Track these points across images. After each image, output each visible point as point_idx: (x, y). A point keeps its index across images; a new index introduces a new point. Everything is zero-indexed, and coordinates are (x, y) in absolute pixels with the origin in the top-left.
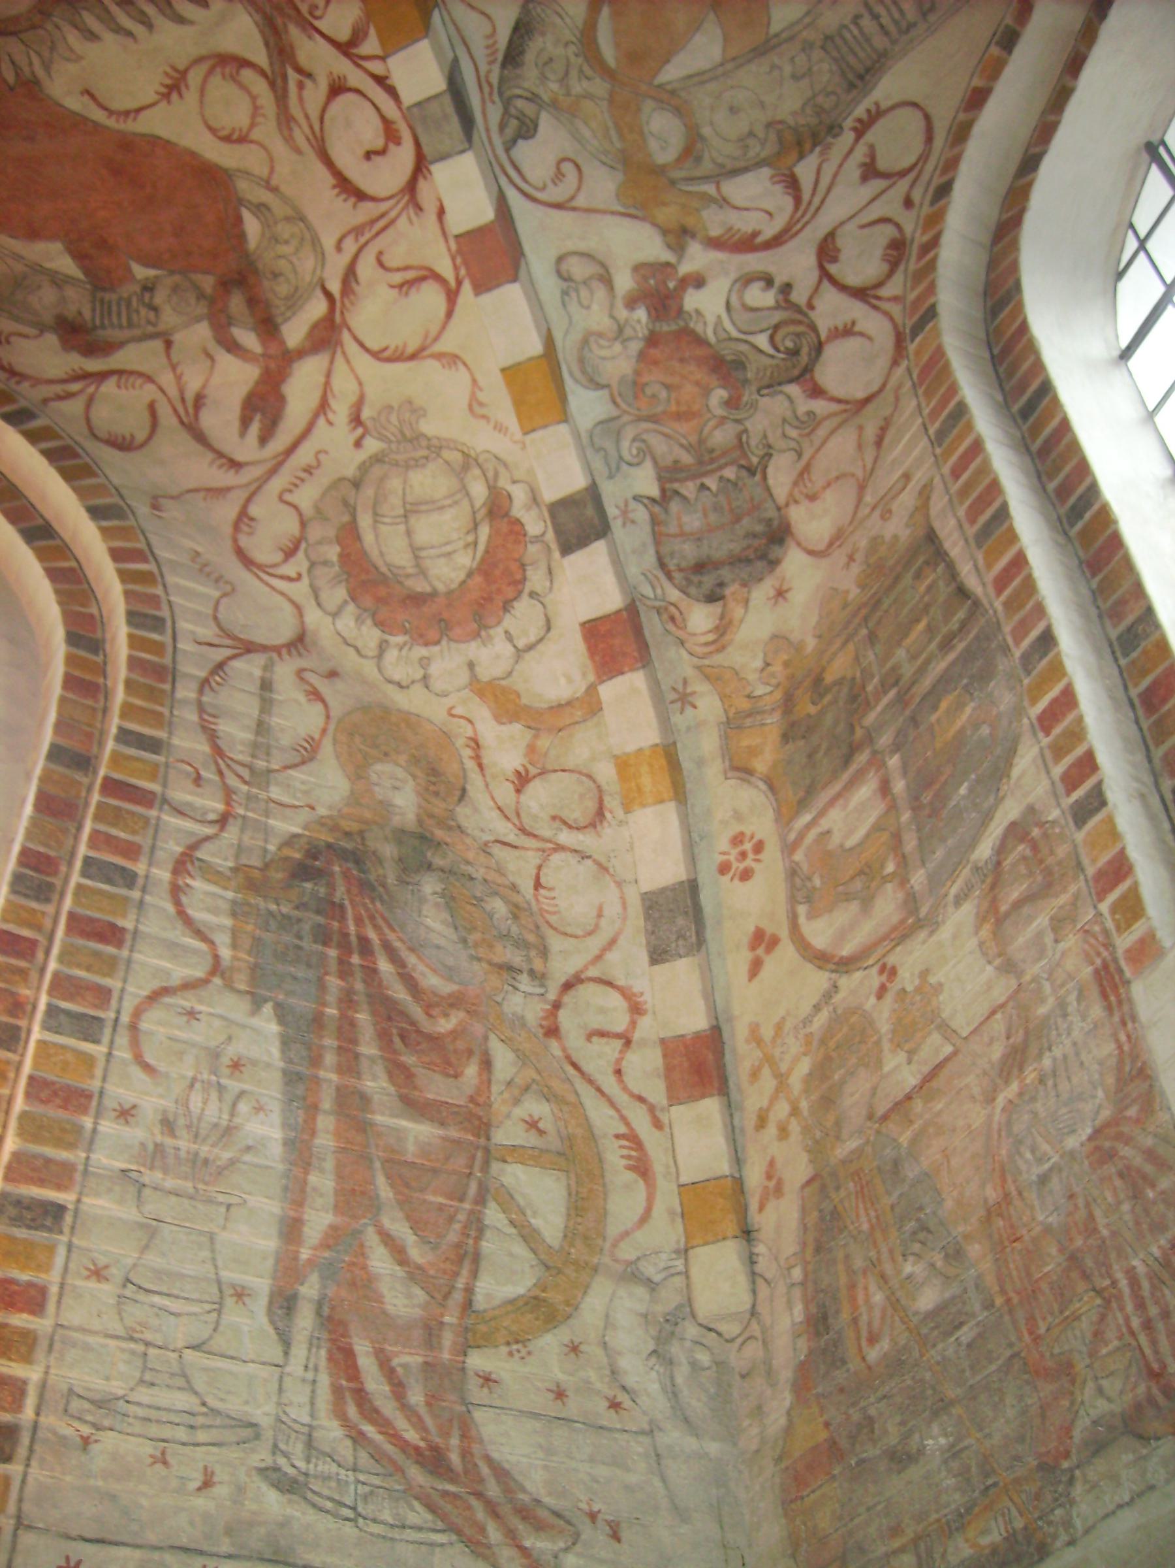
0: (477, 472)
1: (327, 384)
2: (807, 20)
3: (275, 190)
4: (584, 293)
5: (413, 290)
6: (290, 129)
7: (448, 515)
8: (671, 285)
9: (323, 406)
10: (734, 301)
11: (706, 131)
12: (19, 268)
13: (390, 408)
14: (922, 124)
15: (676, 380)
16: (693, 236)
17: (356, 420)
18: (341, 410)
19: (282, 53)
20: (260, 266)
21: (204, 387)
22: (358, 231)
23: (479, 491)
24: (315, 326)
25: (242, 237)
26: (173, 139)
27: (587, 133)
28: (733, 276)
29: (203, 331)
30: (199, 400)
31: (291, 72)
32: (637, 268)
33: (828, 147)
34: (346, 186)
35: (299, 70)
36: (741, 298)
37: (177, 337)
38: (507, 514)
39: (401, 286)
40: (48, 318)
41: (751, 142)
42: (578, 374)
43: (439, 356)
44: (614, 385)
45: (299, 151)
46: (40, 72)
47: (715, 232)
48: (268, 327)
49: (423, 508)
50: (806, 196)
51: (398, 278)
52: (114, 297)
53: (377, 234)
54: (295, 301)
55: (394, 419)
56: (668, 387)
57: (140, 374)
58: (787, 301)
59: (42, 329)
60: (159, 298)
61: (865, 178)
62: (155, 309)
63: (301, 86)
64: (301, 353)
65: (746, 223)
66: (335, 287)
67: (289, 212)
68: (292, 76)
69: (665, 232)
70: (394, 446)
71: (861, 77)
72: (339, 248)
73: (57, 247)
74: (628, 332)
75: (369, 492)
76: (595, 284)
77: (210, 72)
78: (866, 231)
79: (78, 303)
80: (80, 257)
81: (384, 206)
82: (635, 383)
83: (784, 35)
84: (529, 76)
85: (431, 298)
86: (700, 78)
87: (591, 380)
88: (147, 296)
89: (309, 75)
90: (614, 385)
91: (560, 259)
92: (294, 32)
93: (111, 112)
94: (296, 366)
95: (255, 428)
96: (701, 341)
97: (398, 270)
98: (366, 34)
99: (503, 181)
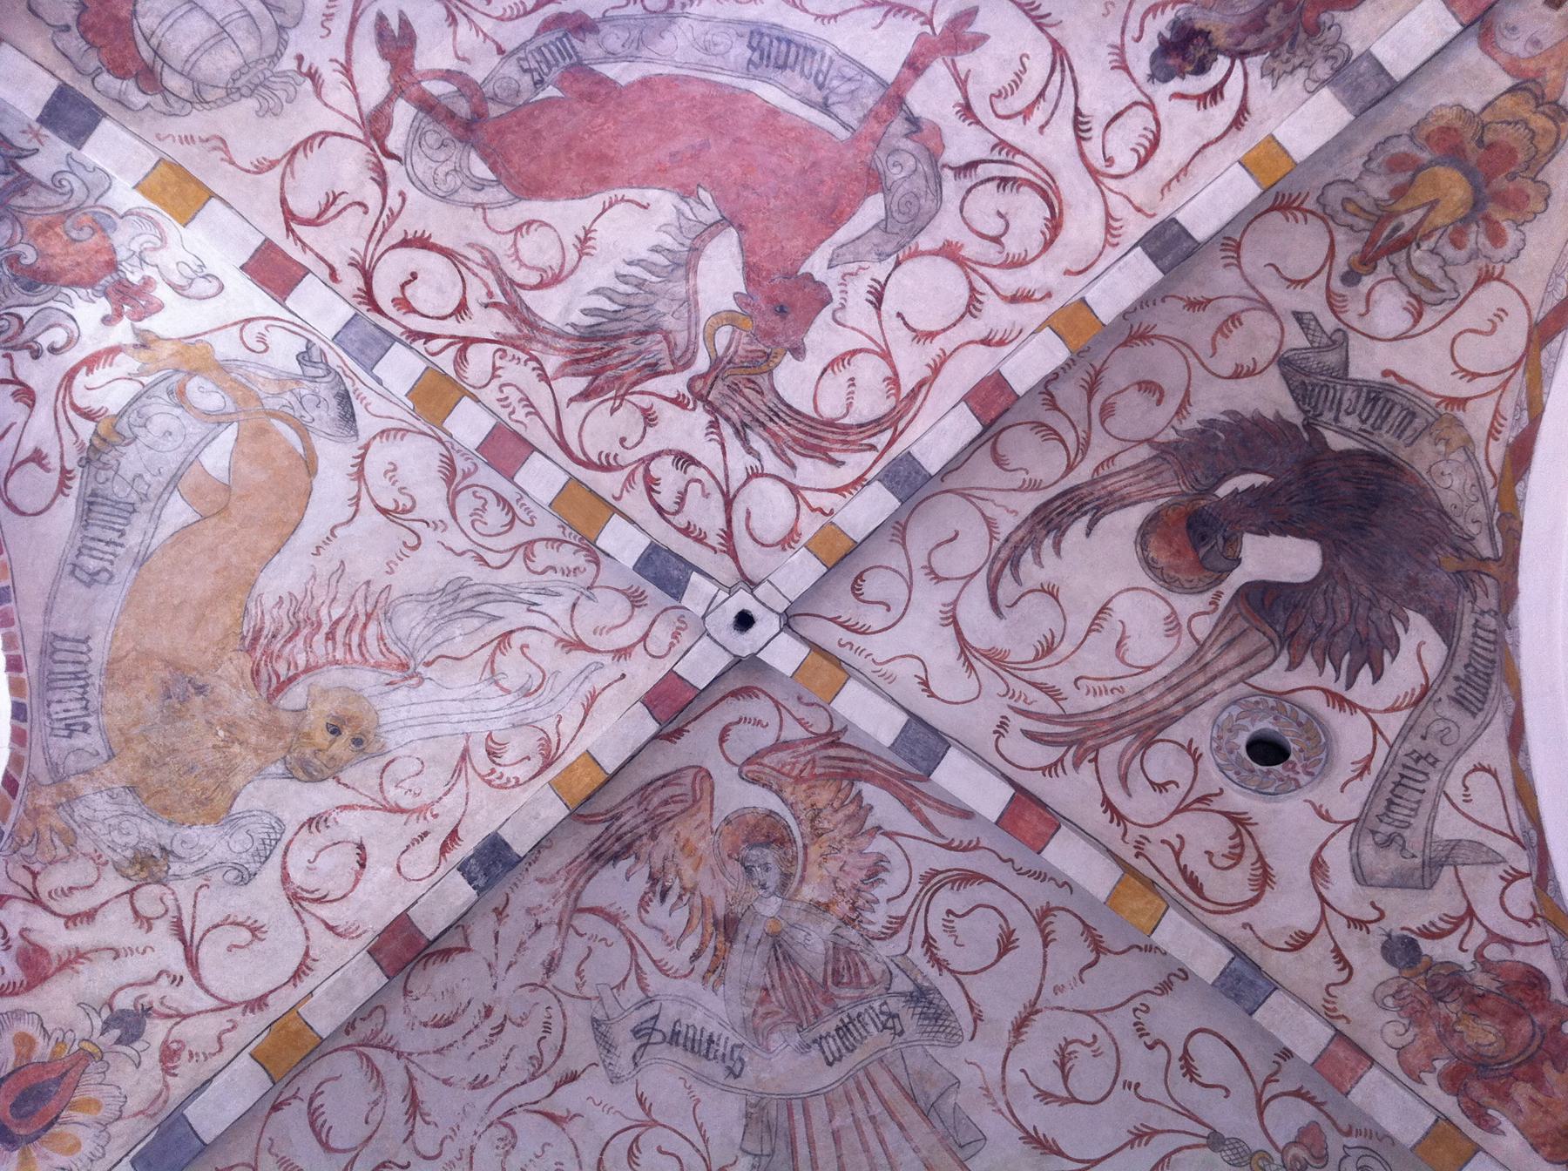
0: (185, 95)
1: (354, 89)
2: (157, 512)
3: (475, 206)
4: (189, 273)
5: (323, 202)
6: (484, 258)
7: (186, 48)
8: (126, 308)
9: (347, 70)
10: (71, 325)
11: (178, 411)
12: (645, 53)
13: (290, 101)
14: (23, 509)
15: (71, 249)
16: (135, 346)
17: (313, 76)
18: (331, 76)
19: (514, 309)
20: (459, 145)
21: (455, 33)
22: (393, 217)
23: (173, 82)
24: (389, 126)
25: (485, 157)
26: (570, 203)
27: (261, 372)
28: (83, 339)
29: (478, 74)
30: (453, 21)
31: (502, 300)
32: (161, 307)
33: (81, 450)
34: (421, 243)
35: (496, 305)
36: (66, 328)
37: (497, 59)
38: (136, 76)
39: (335, 198)
40: (605, 28)
41: (141, 422)
42: (151, 214)
43: (273, 165)
44: (118, 221)
45: (471, 245)
46: (686, 209)
47: (120, 357)
48: (427, 106)
49: (212, 42)
50: (71, 414)
51: (341, 203)
52: (562, 64)
53: (376, 224)
54: (416, 134)
55: (282, 95)
56: (75, 240)
57: (510, 19)
58: (29, 348)
59: (605, 18)
60: (526, 80)
61: (37, 451)
62: (525, 71)
63: (490, 294)
64: (389, 100)
65: (101, 374)
66: (389, 165)
67: (456, 197)
68: (501, 299)
69: (158, 338)
70: (268, 74)
71: (91, 503)
72: (402, 194)
73: (623, 81)
74: (136, 261)
75: (267, 28)
76: (183, 282)
77: (562, 266)
78: (6, 425)
79: (588, 48)
80: (603, 81)
81: (382, 247)
82: (103, 230)
83: (165, 496)
84: (324, 390)
85: (305, 205)
86: (207, 441)
87: (138, 215)
88: (537, 77)
89: (486, 306)
90: (118, 221)
91: (222, 288)
92: (510, 329)
93: (622, 200)
94: (388, 88)
95: (394, 24)
96: (72, 284)
97: (345, 209)
98: (455, 362)
99: (298, 322)
